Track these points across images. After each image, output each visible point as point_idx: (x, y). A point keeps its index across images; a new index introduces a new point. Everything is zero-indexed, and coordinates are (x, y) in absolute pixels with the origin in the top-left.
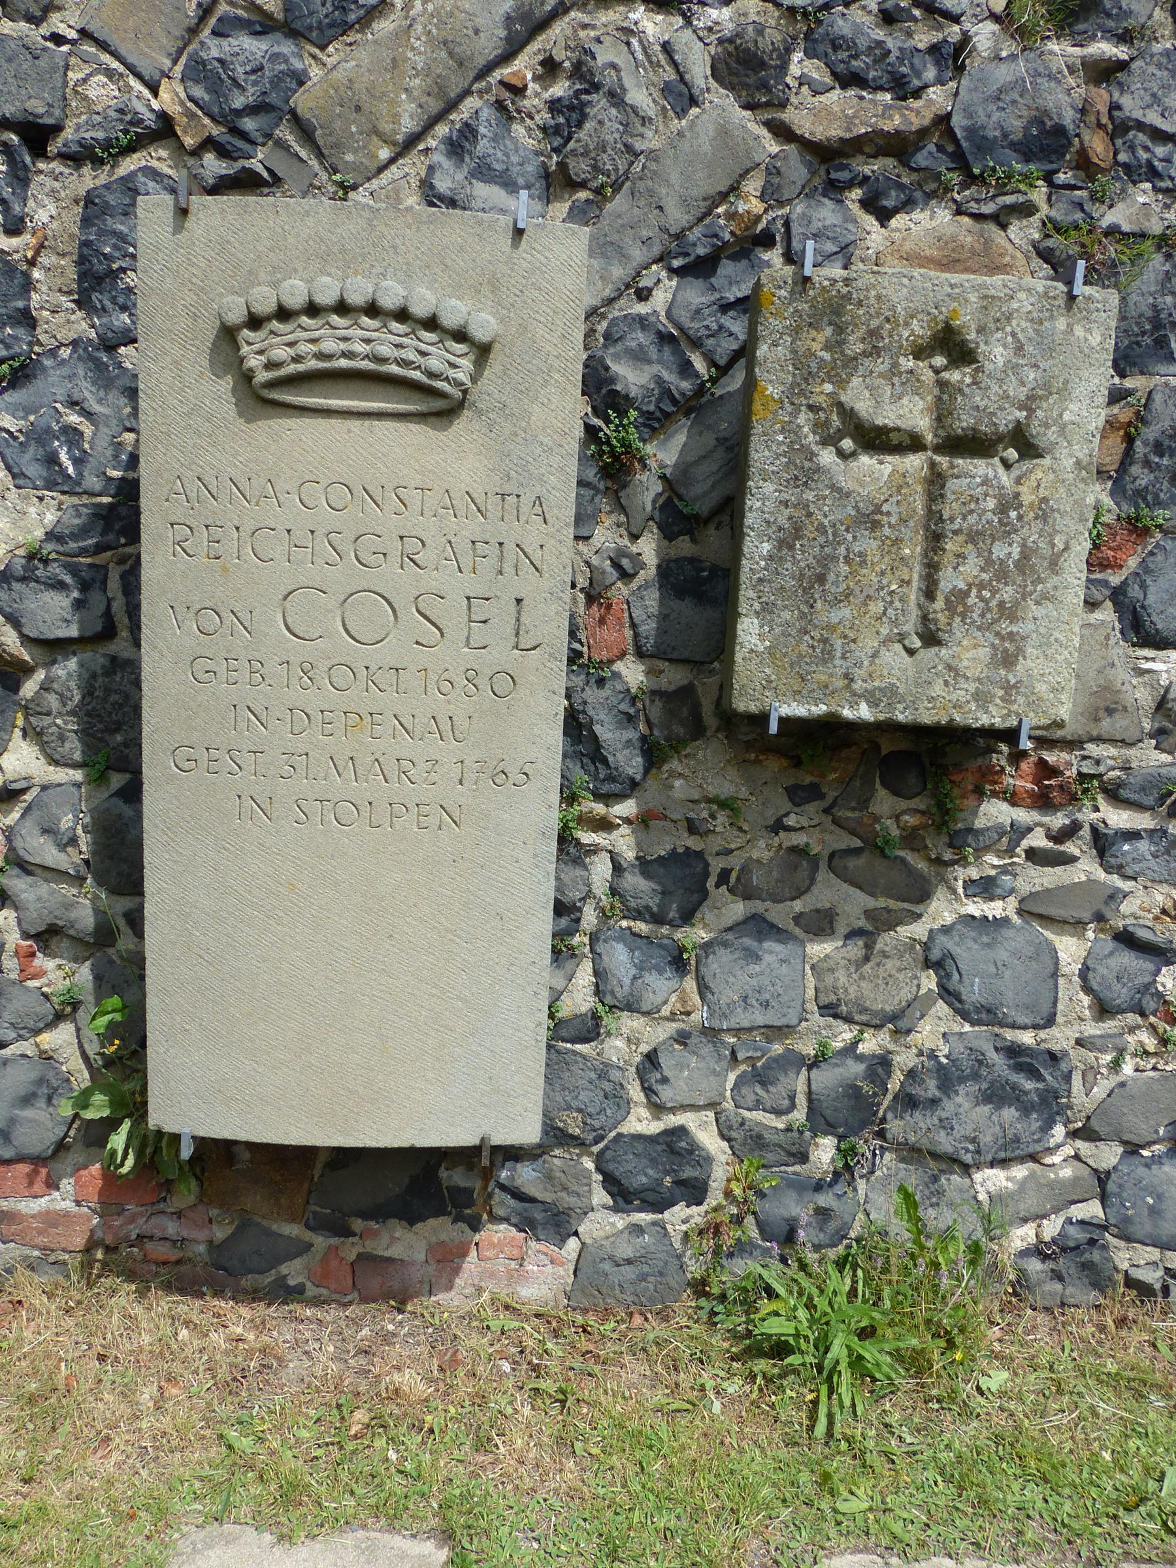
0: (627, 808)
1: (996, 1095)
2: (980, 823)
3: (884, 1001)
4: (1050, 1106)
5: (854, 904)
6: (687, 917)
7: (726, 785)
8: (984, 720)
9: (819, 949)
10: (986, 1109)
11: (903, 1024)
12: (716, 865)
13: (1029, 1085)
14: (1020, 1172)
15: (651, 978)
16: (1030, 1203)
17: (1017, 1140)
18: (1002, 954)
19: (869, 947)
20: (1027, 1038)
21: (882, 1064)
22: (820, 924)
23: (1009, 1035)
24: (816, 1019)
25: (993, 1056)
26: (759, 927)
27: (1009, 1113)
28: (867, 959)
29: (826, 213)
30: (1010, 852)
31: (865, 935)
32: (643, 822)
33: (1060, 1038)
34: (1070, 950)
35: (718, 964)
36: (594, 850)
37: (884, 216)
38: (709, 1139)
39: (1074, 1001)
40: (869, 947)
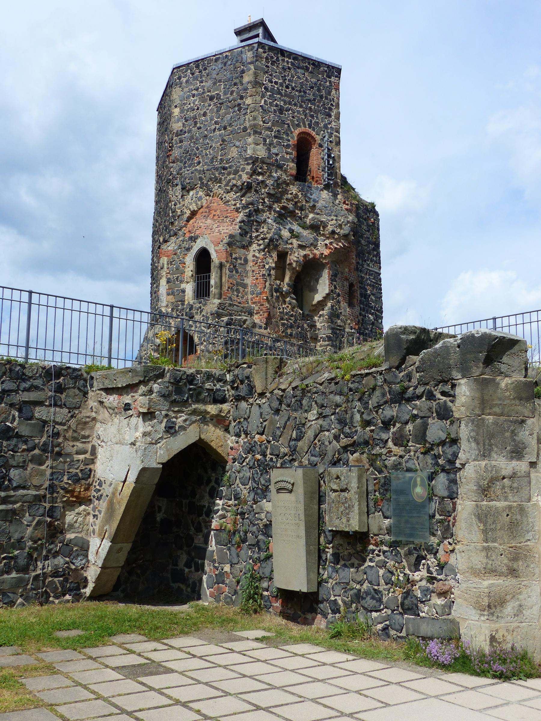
0: (331, 545)
1: (373, 598)
2: (369, 549)
3: (359, 579)
4: (380, 601)
5: (356, 562)
6: (338, 564)
7: (341, 542)
8: (346, 530)
9: (352, 570)
10: (371, 600)
11: (361, 583)
12: (341, 555)
13: (377, 596)
14: (378, 614)
15: (333, 573)
16: (379, 620)
17: (375, 606)
18: (372, 572)
19: (358, 570)
20: (376, 587)
21: (360, 590)
22: (352, 566)
23: (374, 587)
24: (351, 582)
25: (372, 590)
26: (345, 566)
27: (375, 601)
28: (357, 572)
29: (345, 456)
30: (373, 554)
31: (357, 568)
32: (333, 547)
33: (381, 588)
34: (381, 572)
35: (340, 571)
36: (328, 552)
37: (352, 455)
38: (340, 602)
39: (382, 582)
40: (358, 570)
